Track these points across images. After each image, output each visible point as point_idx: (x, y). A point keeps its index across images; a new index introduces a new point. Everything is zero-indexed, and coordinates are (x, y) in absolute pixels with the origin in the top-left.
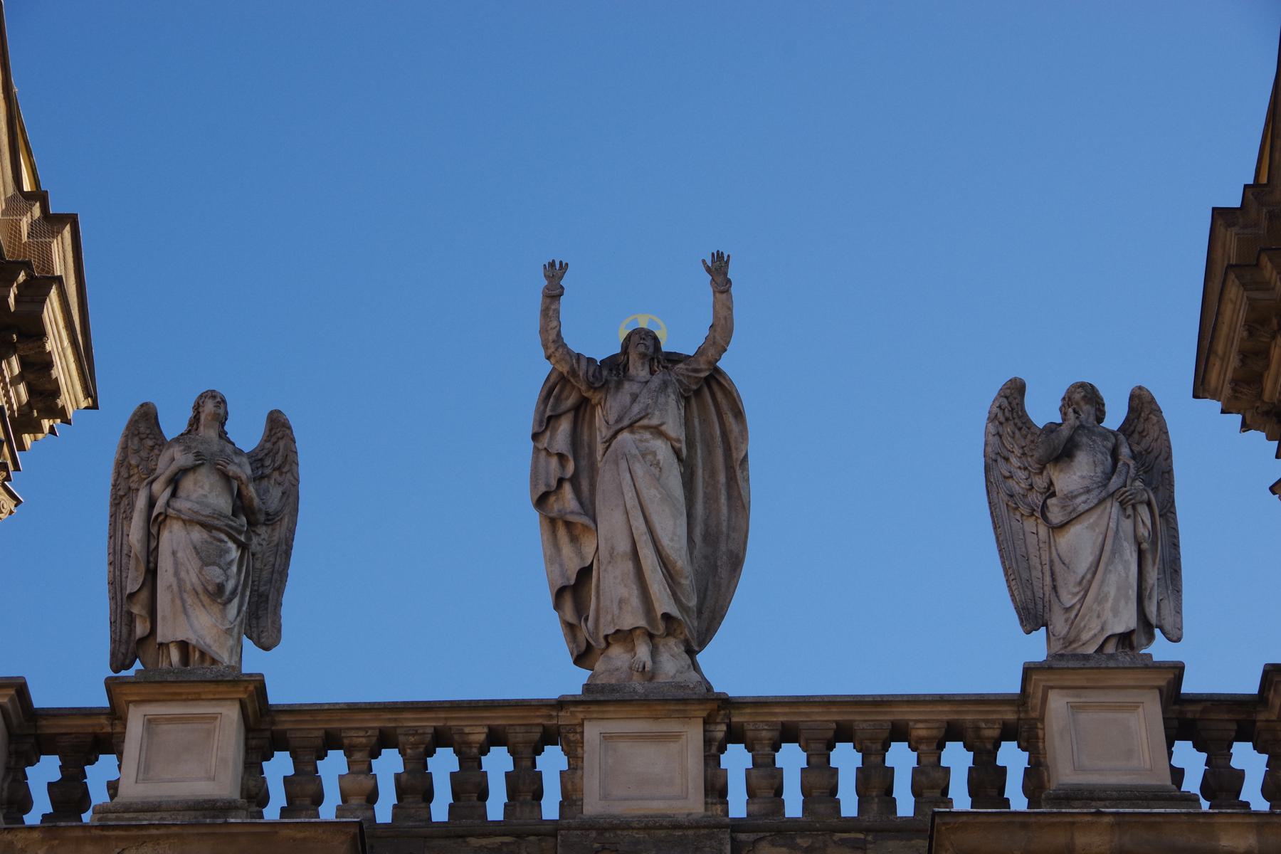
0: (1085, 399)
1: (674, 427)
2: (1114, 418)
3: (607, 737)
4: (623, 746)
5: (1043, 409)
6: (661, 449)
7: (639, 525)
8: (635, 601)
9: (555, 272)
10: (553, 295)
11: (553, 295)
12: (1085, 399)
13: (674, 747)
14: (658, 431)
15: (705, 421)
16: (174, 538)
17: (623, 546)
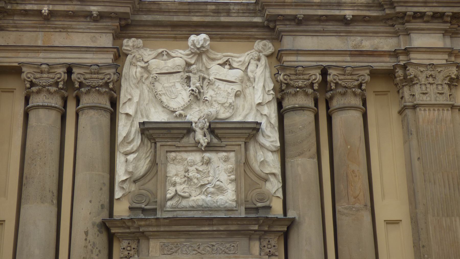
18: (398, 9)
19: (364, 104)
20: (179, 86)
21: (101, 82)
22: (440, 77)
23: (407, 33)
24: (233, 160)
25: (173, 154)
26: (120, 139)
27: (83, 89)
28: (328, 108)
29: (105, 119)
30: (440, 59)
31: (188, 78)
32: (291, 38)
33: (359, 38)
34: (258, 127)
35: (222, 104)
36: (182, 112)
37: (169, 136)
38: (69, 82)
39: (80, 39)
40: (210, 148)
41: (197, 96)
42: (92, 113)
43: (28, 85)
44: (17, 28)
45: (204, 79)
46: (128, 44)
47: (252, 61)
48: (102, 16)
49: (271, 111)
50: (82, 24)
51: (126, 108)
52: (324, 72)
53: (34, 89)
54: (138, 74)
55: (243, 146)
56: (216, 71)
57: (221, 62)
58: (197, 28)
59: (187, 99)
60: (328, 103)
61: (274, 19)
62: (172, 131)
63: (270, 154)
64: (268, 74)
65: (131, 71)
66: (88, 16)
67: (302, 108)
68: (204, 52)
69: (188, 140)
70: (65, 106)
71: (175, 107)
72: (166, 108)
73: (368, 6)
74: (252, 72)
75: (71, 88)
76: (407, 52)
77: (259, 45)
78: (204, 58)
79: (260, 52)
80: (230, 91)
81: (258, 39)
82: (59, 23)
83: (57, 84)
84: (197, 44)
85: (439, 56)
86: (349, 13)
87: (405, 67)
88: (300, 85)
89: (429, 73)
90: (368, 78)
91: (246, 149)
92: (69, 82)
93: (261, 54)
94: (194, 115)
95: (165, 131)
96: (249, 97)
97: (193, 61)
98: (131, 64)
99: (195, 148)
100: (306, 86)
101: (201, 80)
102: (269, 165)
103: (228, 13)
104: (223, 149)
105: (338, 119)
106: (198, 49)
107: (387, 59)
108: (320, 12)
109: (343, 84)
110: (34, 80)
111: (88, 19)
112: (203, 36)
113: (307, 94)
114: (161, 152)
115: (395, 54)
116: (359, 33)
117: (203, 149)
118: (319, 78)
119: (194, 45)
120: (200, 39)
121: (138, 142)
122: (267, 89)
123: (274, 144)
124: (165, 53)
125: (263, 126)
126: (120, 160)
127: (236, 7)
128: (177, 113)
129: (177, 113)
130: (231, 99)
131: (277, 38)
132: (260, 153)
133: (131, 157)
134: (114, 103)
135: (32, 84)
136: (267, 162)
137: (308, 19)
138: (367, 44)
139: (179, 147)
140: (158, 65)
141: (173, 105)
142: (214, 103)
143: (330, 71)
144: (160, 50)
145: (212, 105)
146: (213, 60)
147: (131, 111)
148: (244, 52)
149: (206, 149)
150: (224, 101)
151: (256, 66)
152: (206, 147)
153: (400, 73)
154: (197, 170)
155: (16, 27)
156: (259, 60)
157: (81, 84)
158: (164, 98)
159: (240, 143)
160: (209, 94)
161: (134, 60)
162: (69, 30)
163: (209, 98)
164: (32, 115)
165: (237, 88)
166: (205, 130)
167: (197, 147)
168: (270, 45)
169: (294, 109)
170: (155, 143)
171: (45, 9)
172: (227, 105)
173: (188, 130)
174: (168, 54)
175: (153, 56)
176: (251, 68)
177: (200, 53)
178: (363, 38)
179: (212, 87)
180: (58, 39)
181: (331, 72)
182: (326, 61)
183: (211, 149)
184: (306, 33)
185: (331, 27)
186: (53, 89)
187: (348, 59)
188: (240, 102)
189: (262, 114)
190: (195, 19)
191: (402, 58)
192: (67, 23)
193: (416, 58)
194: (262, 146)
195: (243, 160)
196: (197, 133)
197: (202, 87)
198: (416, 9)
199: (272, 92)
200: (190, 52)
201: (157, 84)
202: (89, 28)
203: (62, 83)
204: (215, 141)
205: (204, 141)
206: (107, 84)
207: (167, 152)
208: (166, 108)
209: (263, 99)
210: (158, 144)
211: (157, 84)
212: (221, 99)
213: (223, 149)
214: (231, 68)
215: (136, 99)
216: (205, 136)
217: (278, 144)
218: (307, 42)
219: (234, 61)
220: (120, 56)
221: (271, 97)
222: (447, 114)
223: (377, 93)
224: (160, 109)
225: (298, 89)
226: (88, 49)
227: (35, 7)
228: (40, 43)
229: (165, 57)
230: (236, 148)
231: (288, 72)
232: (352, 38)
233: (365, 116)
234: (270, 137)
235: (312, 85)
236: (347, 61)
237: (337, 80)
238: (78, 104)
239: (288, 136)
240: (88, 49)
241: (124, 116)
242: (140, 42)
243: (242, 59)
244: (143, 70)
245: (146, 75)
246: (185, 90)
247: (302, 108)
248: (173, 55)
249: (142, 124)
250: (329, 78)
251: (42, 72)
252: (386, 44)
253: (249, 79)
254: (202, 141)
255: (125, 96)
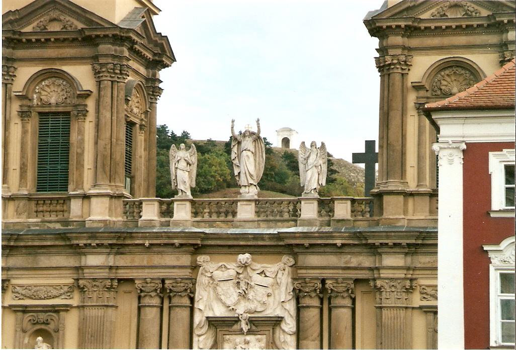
0: (313, 144)
1: (253, 150)
2: (319, 145)
3: (241, 204)
4: (244, 206)
5: (308, 145)
6: (249, 154)
7: (246, 168)
8: (246, 180)
9: (233, 121)
10: (232, 128)
11: (232, 128)
12: (313, 144)
13: (250, 206)
14: (249, 150)
15: (258, 144)
16: (178, 170)
17: (244, 172)
18: (370, 241)
19: (354, 301)
20: (232, 288)
21: (182, 289)
22: (399, 286)
23: (380, 254)
24: (264, 340)
25: (228, 337)
26: (195, 326)
27: (171, 294)
28: (330, 303)
29: (185, 313)
30: (400, 274)
31: (238, 283)
32: (304, 256)
33: (349, 256)
34: (280, 319)
35: (259, 302)
36: (233, 307)
37: (224, 325)
38: (163, 289)
39: (170, 259)
40: (250, 332)
41: (244, 296)
42: (177, 309)
43: (139, 292)
44: (131, 253)
45: (248, 284)
46: (201, 259)
47: (279, 272)
48: (181, 245)
49: (291, 307)
50: (170, 249)
51: (199, 305)
52: (323, 281)
53: (142, 294)
54: (207, 282)
55: (271, 331)
56: (257, 279)
57: (259, 272)
58: (243, 249)
59: (236, 298)
60: (330, 299)
61: (291, 245)
62: (226, 322)
63: (289, 336)
64: (290, 280)
65: (202, 280)
66: (173, 244)
67: (308, 307)
68: (249, 266)
69: (236, 327)
70: (162, 303)
71: (229, 304)
72: (224, 304)
73: (349, 238)
74: (280, 278)
75: (165, 292)
76: (378, 269)
77: (285, 258)
78: (249, 269)
79: (285, 264)
80: (264, 292)
81: (285, 254)
82: (155, 249)
83: (156, 290)
84: (242, 261)
85: (401, 271)
86: (339, 242)
87: (374, 280)
88: (307, 291)
89: (392, 284)
90: (353, 286)
91: (273, 333)
92: (163, 289)
93: (286, 265)
94: (240, 310)
95: (221, 322)
96: (277, 297)
97: (241, 272)
98: (202, 274)
99: (240, 332)
100: (311, 291)
101: (246, 284)
102: (288, 344)
103: (263, 239)
104: (259, 333)
105: (335, 312)
106: (244, 264)
107: (367, 272)
108: (319, 242)
109: (335, 290)
110: (142, 289)
111: (174, 247)
112: (247, 255)
113: (311, 297)
114: (220, 334)
115: (371, 269)
116: (349, 253)
117: (245, 334)
118: (320, 286)
119: (241, 262)
120: (244, 257)
121: (206, 327)
122: (288, 292)
123: (290, 330)
124: (223, 266)
125: (286, 318)
126: (195, 339)
127: (267, 236)
128: (231, 308)
129: (231, 308)
130: (265, 299)
131: (295, 255)
132: (282, 336)
133: (201, 338)
134: (192, 300)
135: (142, 291)
136: (287, 342)
137: (311, 245)
138: (354, 261)
139: (231, 332)
140: (219, 275)
141: (229, 303)
142: (255, 301)
143: (327, 281)
144: (220, 264)
145: (253, 301)
146: (254, 270)
147: (202, 307)
148: (276, 263)
149: (248, 333)
150: (260, 299)
151: (282, 274)
152: (248, 331)
153: (372, 283)
154: (241, 347)
155: (130, 253)
156: (284, 270)
157: (171, 291)
158: (223, 297)
159: (269, 329)
160: (251, 295)
161: (204, 272)
162: (163, 253)
163: (251, 297)
164: (142, 310)
165: (270, 291)
166: (247, 320)
167: (241, 332)
168: (291, 259)
169: (303, 307)
170: (217, 329)
171: (147, 244)
172: (262, 302)
173: (237, 320)
174: (225, 267)
175: (216, 268)
176: (280, 275)
177: (245, 266)
178: (352, 256)
179: (253, 289)
180: (157, 260)
181: (328, 282)
182: (326, 273)
183: (251, 333)
184: (313, 253)
185: (328, 250)
186: (153, 294)
187: (341, 271)
188: (271, 299)
189: (285, 309)
190: (242, 243)
191: (375, 272)
192: (161, 249)
193: (384, 273)
194: (284, 331)
195: (271, 341)
196: (242, 323)
197: (246, 289)
198: (381, 241)
199: (292, 293)
200: (238, 265)
201: (218, 288)
202: (175, 252)
203: (159, 290)
204: (254, 328)
205: (245, 328)
206: (186, 290)
207: (224, 335)
208: (224, 304)
209: (286, 298)
210: (218, 330)
211: (218, 288)
212: (260, 299)
213: (259, 333)
214: (266, 276)
215: (205, 299)
216: (247, 325)
217: (294, 329)
218: (314, 260)
219: (268, 271)
220: (195, 267)
221: (291, 297)
222: (402, 313)
223: (364, 293)
224: (221, 305)
225: (305, 294)
226: (174, 267)
227: (140, 242)
228: (145, 263)
229: (223, 269)
230: (267, 332)
231: (300, 282)
232: (345, 256)
233: (353, 310)
234: (290, 325)
235: (315, 290)
236: (340, 274)
237: (332, 288)
238: (170, 303)
239: (301, 325)
240: (174, 267)
241: (198, 310)
242: (207, 258)
243: (273, 270)
244: (209, 278)
245: (211, 282)
246: (236, 292)
247: (308, 307)
248: (229, 267)
249: (207, 318)
250: (327, 286)
251: (147, 283)
252: (367, 261)
253: (277, 283)
254: (244, 329)
255: (198, 297)
